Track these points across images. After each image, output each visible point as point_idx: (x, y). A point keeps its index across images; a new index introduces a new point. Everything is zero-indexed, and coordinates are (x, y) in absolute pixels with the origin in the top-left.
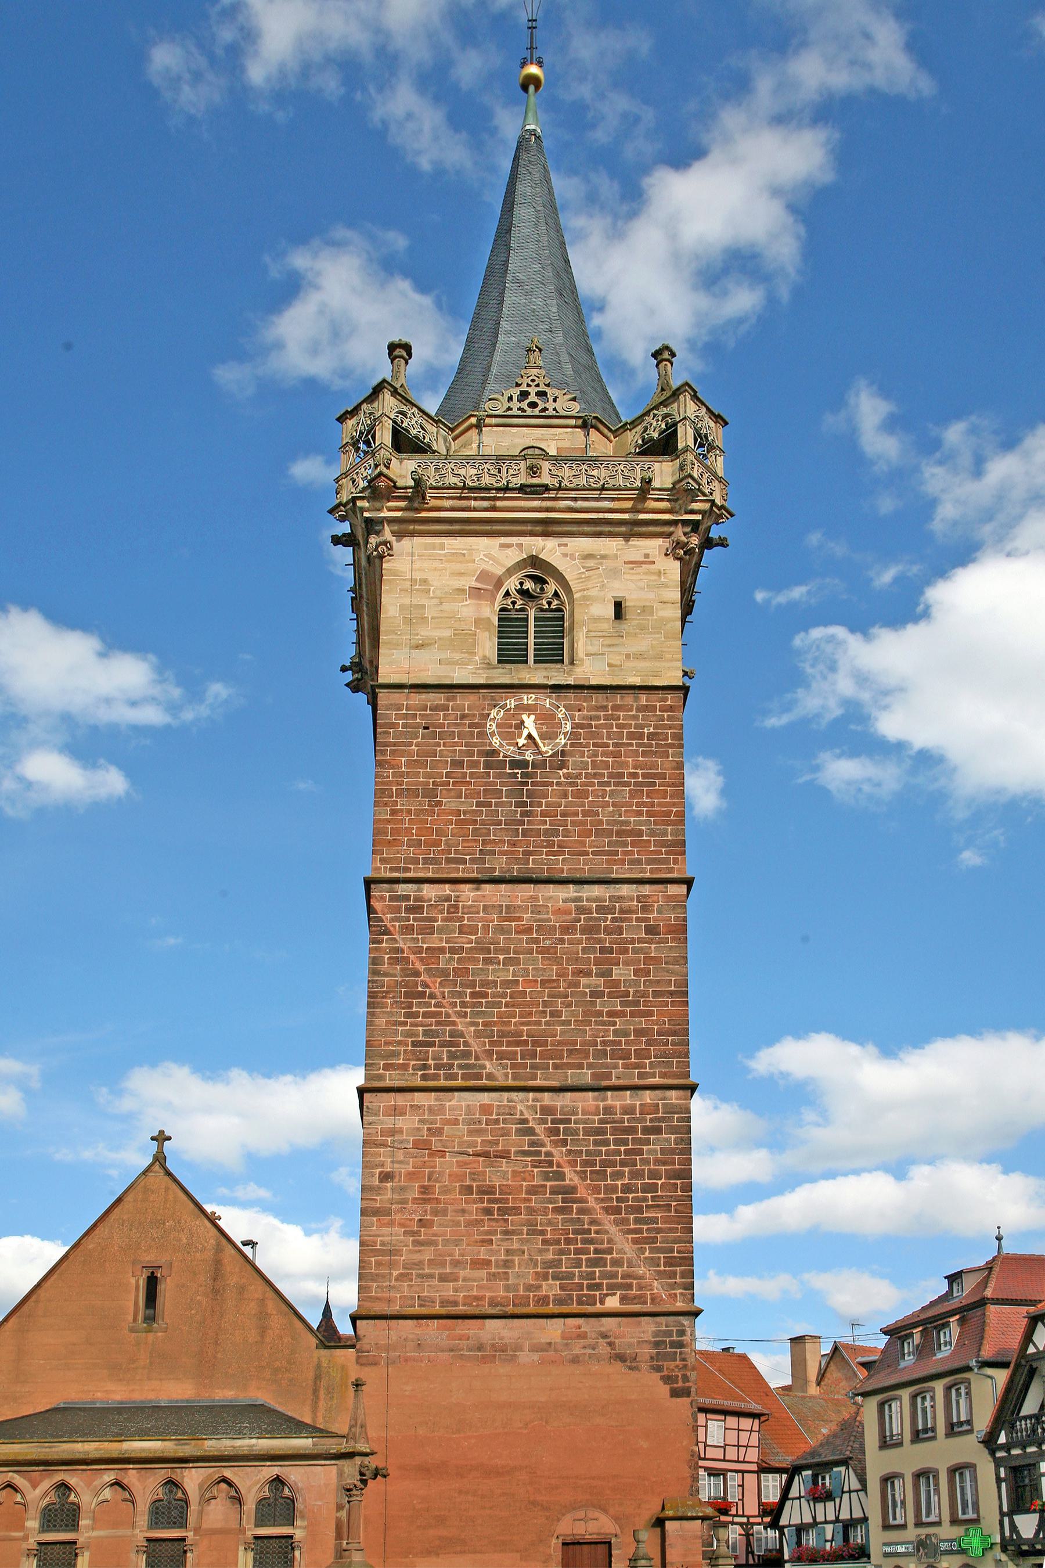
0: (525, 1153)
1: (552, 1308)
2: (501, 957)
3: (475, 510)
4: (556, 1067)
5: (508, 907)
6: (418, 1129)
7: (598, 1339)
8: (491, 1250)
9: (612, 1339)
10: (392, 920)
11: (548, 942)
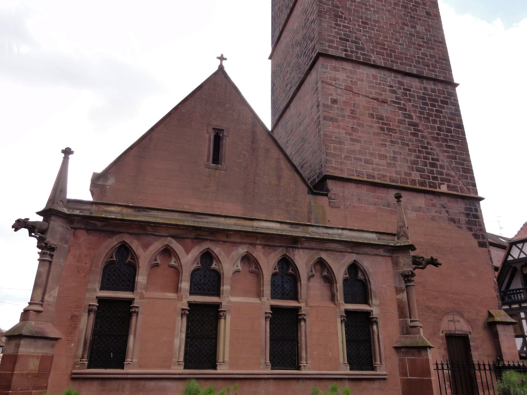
0: (394, 102)
8: (386, 150)
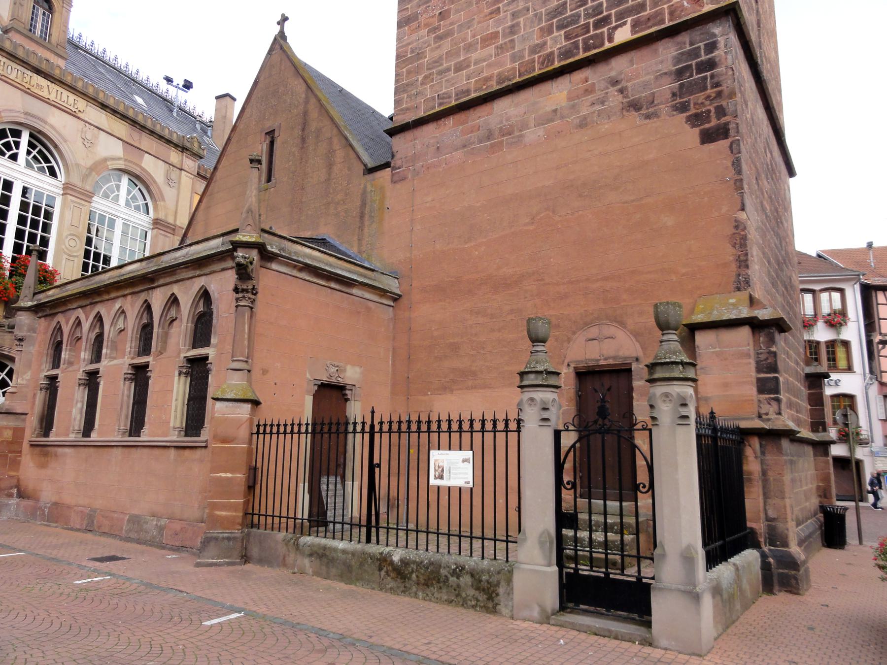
7: (608, 88)
9: (623, 84)
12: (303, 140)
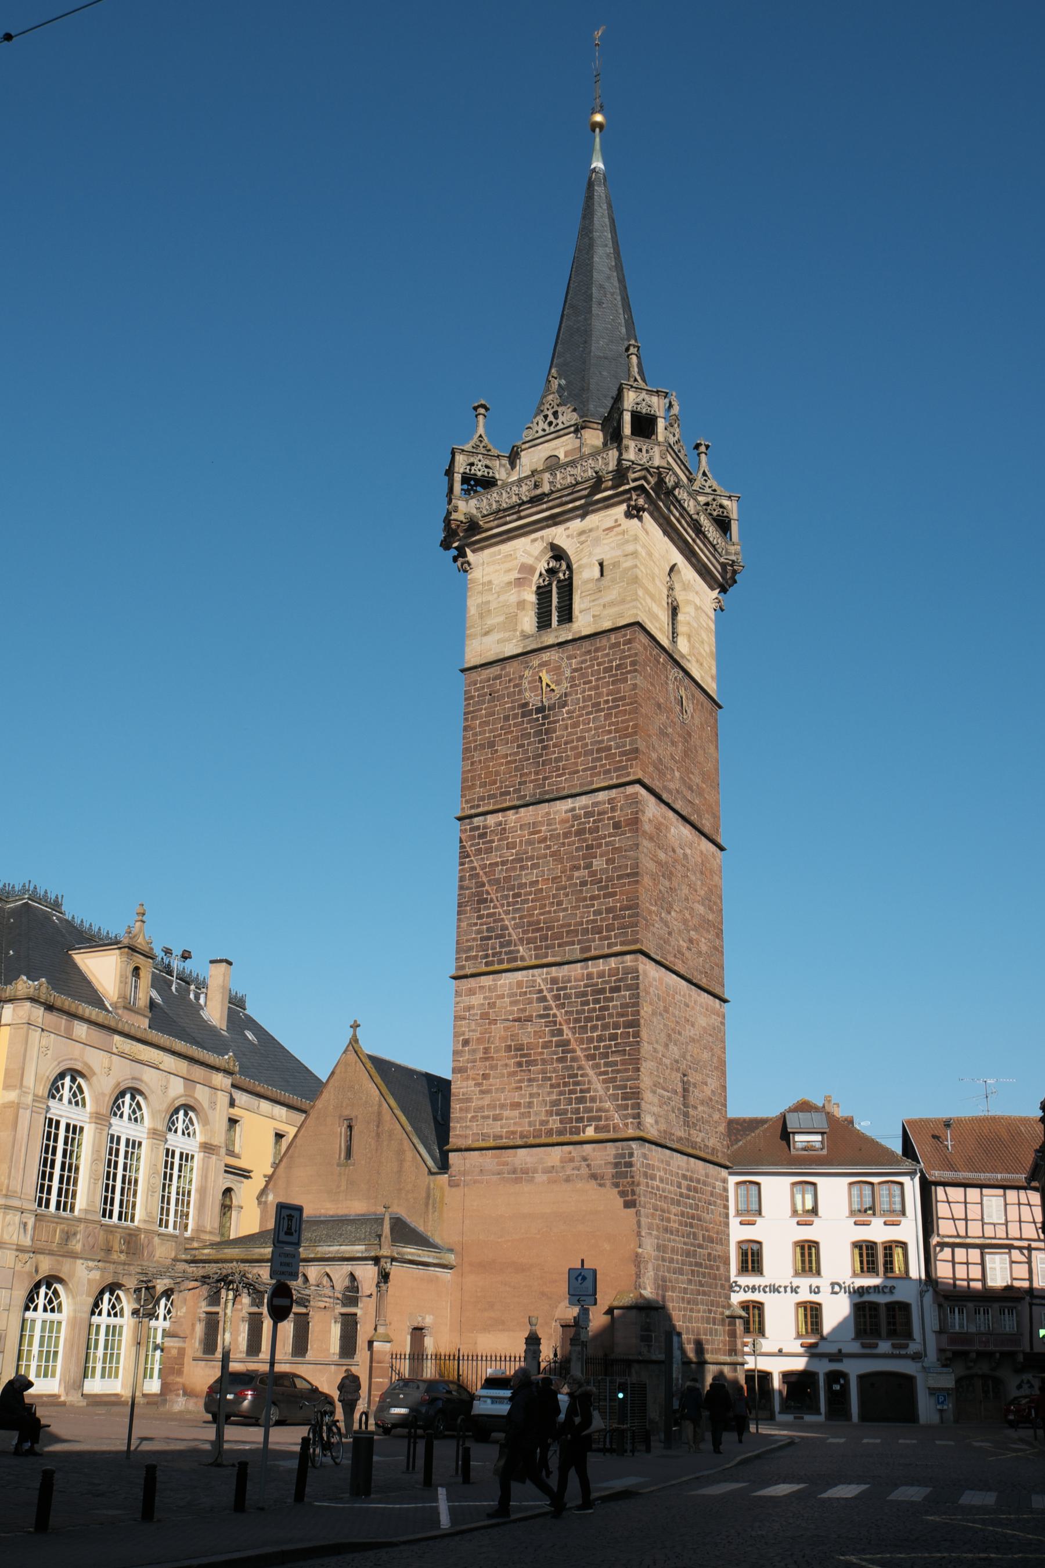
0: (541, 1016)
1: (555, 1139)
2: (529, 863)
3: (511, 522)
4: (560, 945)
5: (534, 823)
6: (483, 1004)
8: (521, 1095)
9: (589, 1162)
10: (472, 845)
11: (556, 847)
12: (378, 1135)
